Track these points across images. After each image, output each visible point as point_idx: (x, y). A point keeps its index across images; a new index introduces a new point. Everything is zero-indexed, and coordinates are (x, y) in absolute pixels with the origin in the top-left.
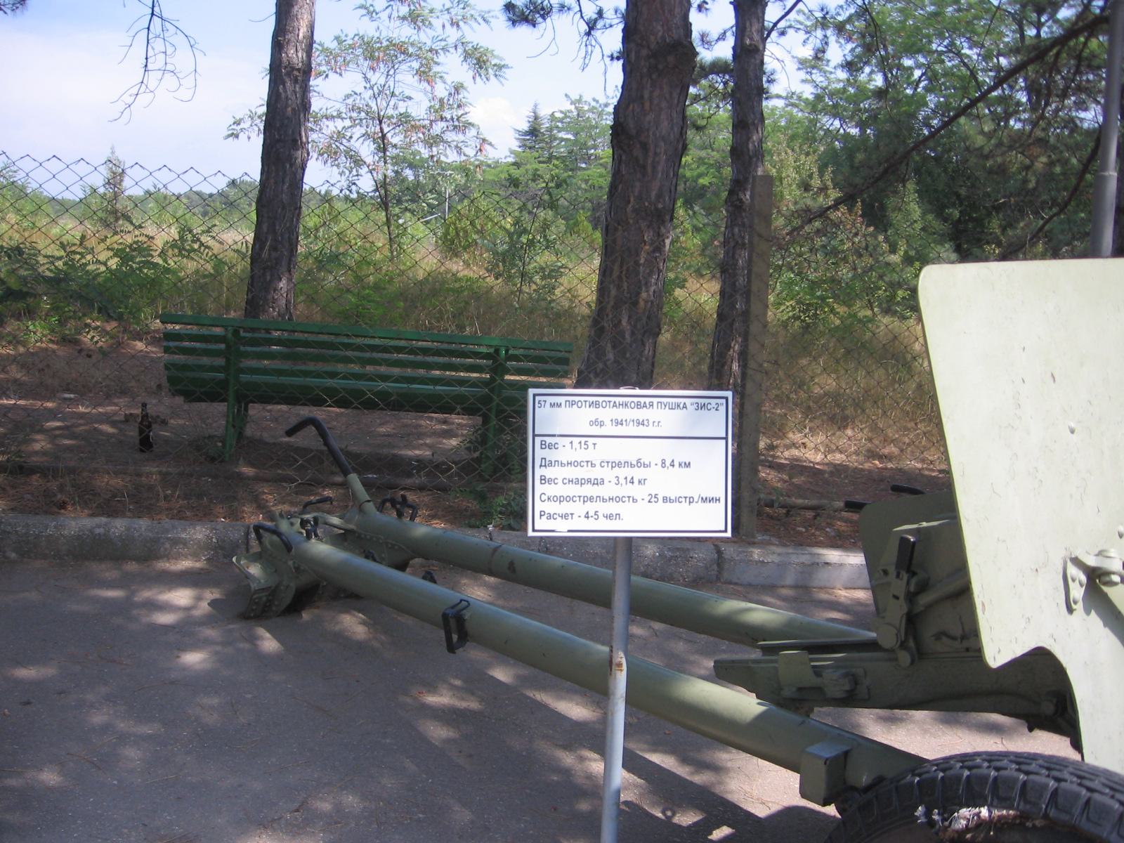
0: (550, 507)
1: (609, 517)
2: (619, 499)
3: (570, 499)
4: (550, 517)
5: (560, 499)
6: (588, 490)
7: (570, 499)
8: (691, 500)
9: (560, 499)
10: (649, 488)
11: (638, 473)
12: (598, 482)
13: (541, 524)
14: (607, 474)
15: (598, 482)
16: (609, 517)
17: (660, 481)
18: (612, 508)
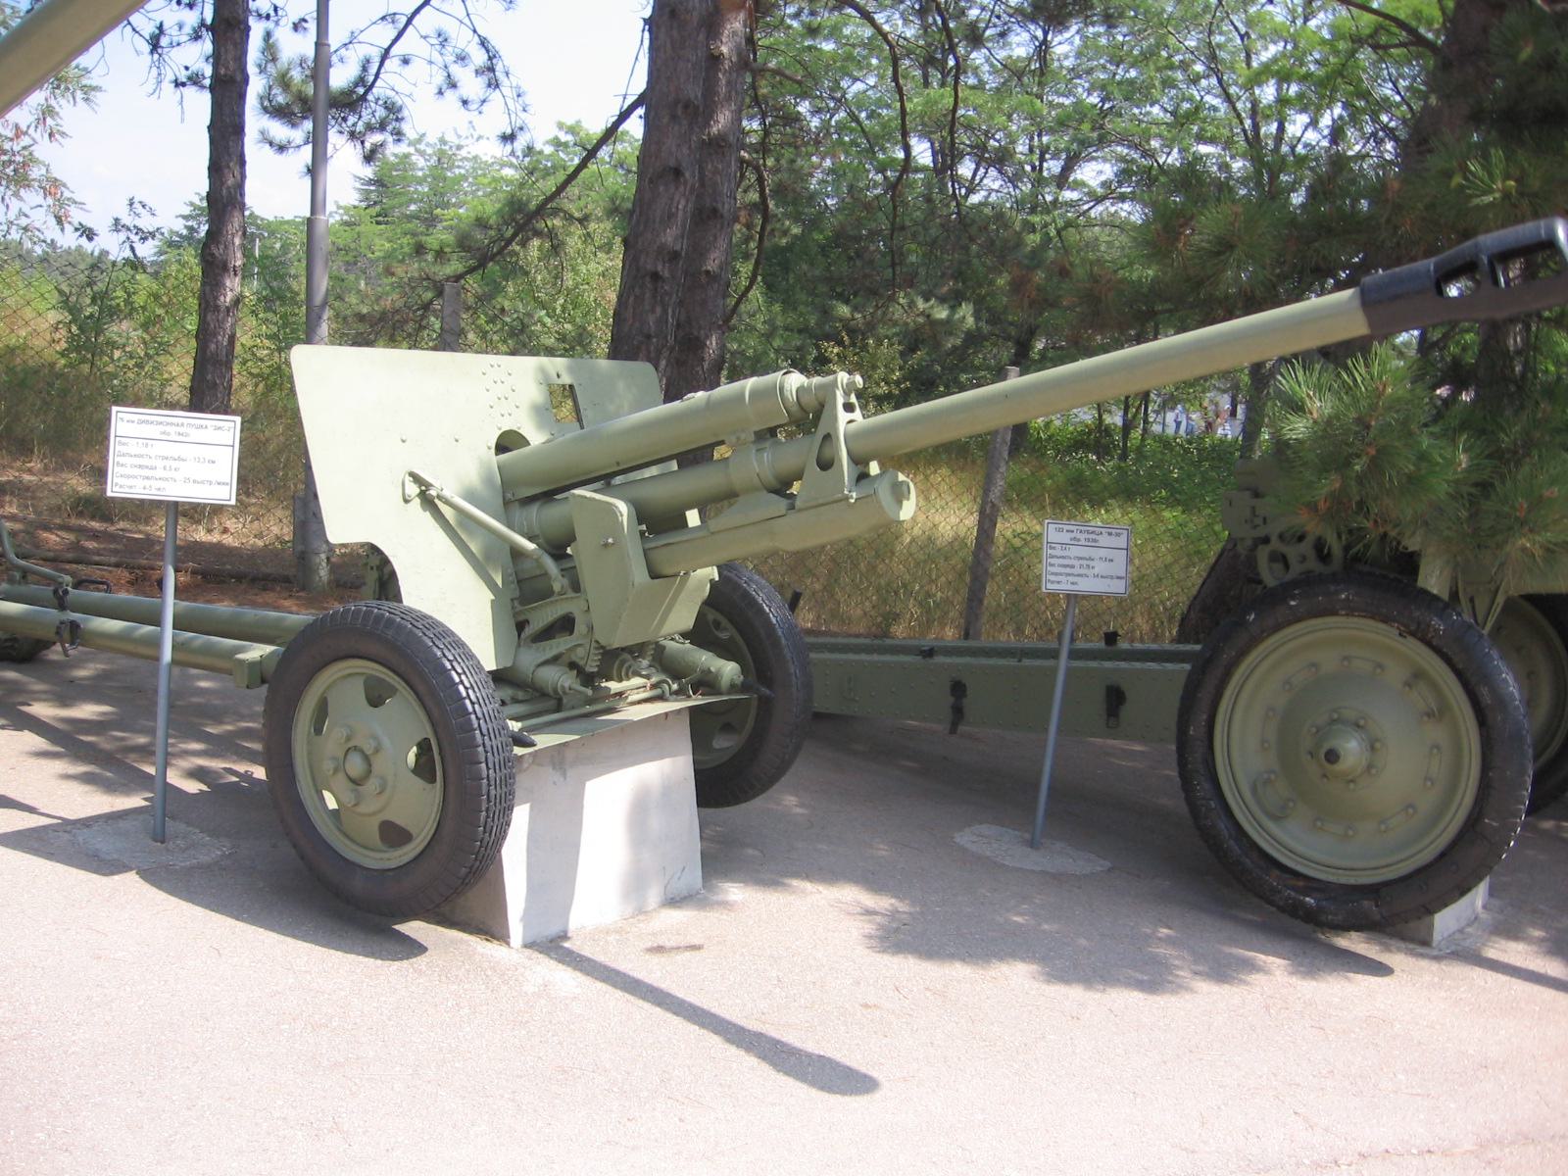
0: (1052, 578)
1: (1072, 583)
2: (1079, 575)
3: (1061, 574)
4: (1053, 582)
5: (1056, 574)
6: (1068, 570)
7: (1061, 574)
8: (1112, 577)
9: (1056, 574)
10: (1096, 571)
11: (1091, 563)
12: (1073, 567)
13: (1049, 586)
14: (1077, 563)
15: (1073, 567)
16: (1072, 583)
17: (1100, 568)
18: (1075, 579)
